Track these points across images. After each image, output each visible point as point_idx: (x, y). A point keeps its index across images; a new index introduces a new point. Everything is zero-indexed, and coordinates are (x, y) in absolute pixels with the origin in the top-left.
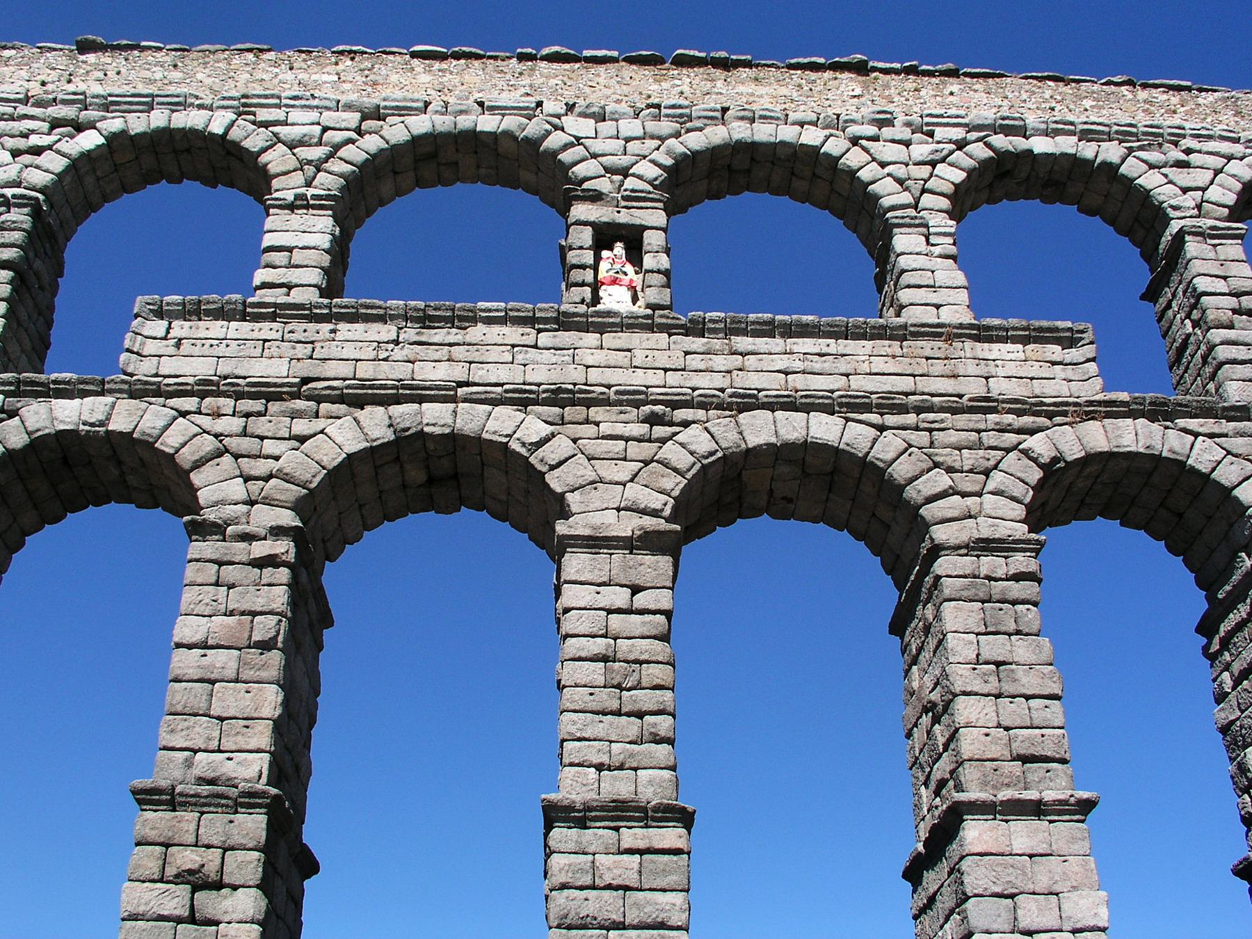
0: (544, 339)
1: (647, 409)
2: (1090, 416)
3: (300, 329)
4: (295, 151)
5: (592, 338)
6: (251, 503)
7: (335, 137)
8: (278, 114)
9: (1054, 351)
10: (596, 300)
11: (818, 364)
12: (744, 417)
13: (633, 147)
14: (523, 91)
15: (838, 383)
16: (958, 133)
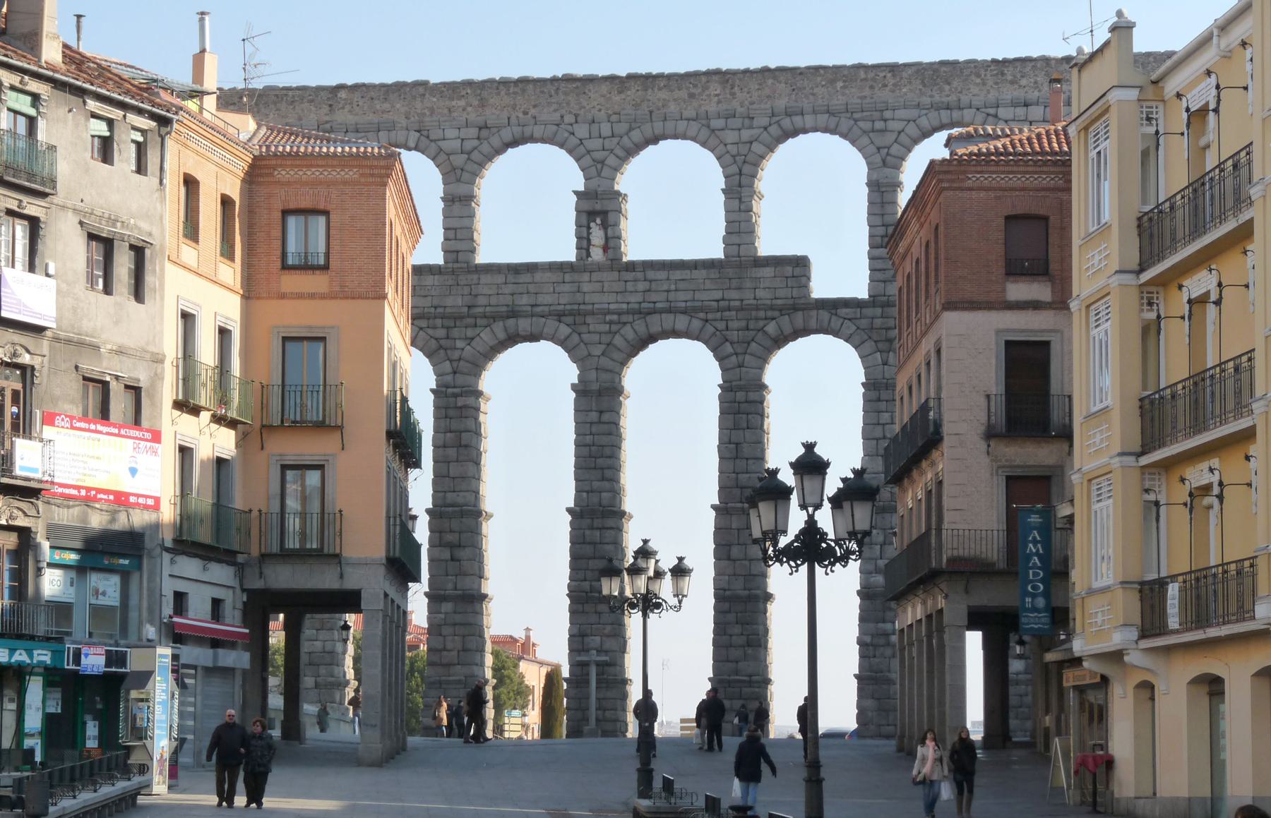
0: (568, 277)
1: (608, 318)
2: (795, 308)
3: (463, 279)
4: (452, 157)
5: (586, 277)
6: (455, 373)
7: (468, 145)
8: (439, 134)
9: (789, 270)
10: (589, 255)
11: (681, 285)
12: (648, 318)
13: (607, 142)
14: (555, 106)
15: (689, 296)
16: (765, 121)
